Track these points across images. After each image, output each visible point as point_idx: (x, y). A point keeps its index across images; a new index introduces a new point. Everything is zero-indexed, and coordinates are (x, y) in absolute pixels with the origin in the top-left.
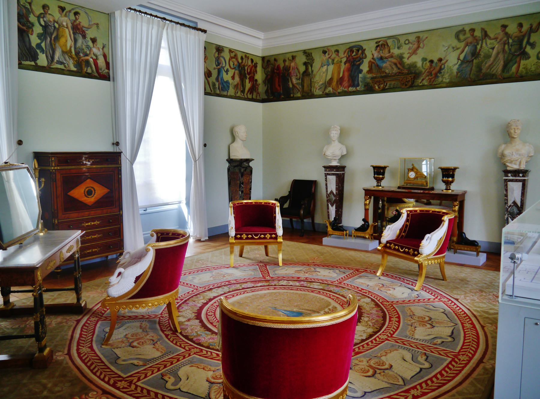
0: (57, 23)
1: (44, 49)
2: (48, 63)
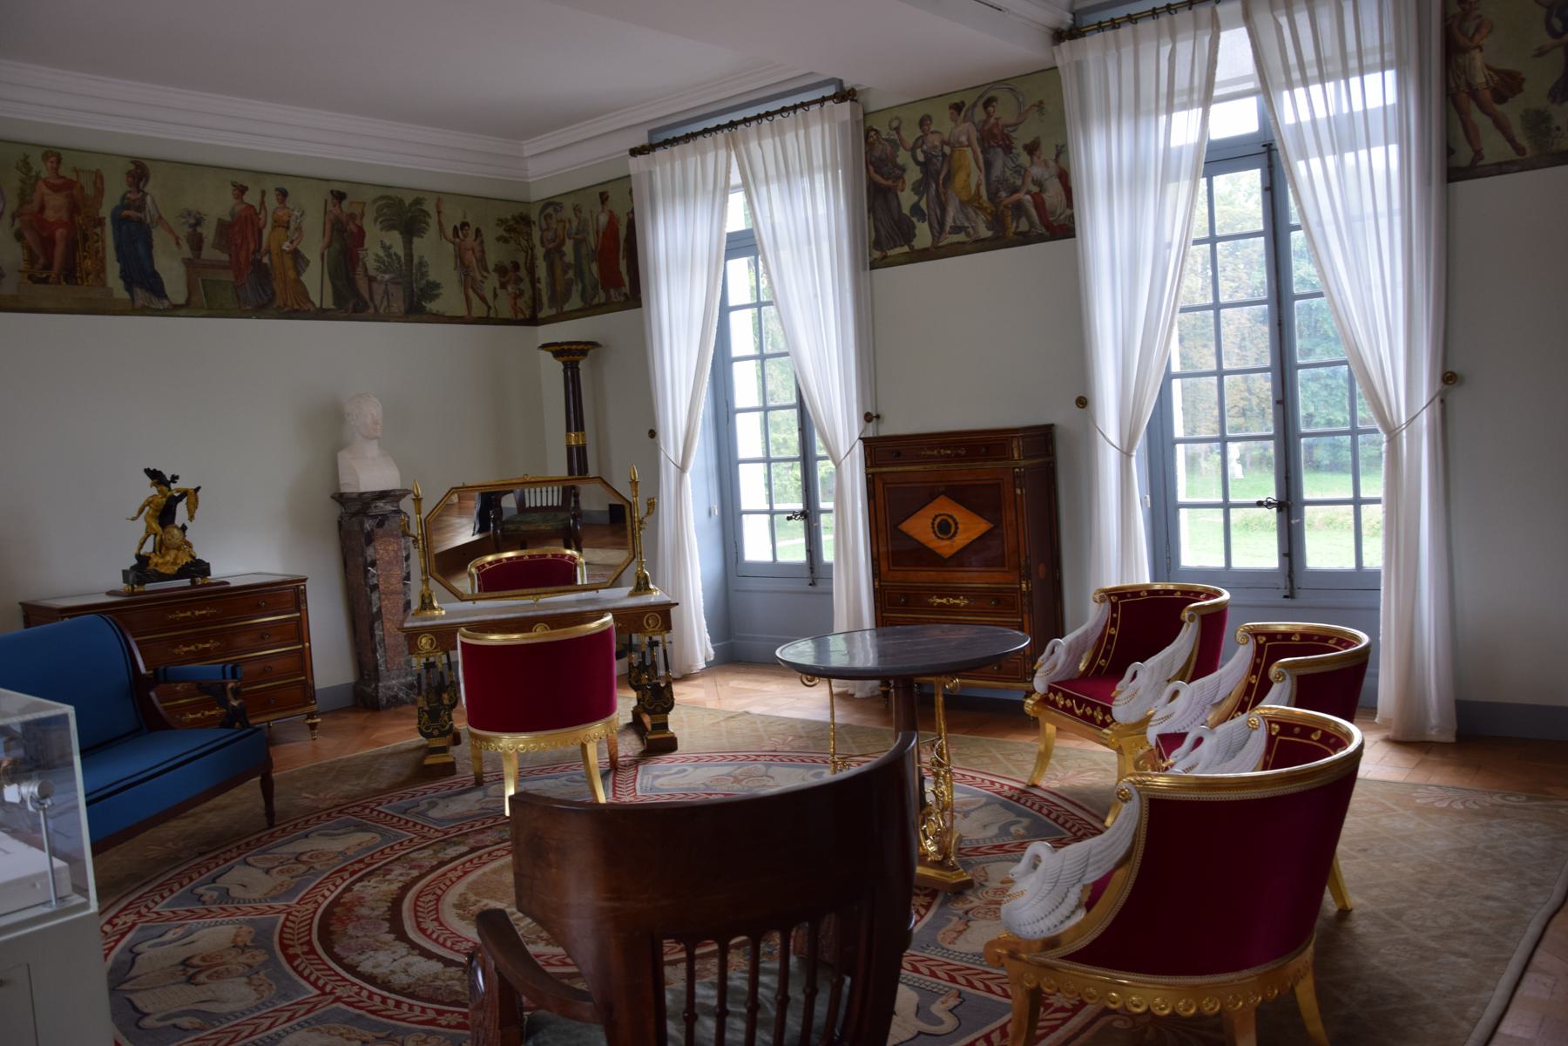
0: (948, 143)
1: (926, 211)
2: (934, 239)
